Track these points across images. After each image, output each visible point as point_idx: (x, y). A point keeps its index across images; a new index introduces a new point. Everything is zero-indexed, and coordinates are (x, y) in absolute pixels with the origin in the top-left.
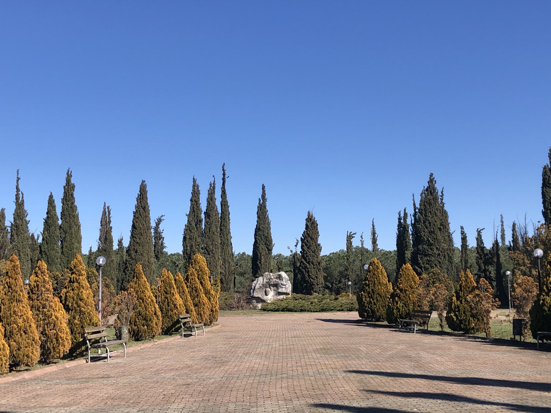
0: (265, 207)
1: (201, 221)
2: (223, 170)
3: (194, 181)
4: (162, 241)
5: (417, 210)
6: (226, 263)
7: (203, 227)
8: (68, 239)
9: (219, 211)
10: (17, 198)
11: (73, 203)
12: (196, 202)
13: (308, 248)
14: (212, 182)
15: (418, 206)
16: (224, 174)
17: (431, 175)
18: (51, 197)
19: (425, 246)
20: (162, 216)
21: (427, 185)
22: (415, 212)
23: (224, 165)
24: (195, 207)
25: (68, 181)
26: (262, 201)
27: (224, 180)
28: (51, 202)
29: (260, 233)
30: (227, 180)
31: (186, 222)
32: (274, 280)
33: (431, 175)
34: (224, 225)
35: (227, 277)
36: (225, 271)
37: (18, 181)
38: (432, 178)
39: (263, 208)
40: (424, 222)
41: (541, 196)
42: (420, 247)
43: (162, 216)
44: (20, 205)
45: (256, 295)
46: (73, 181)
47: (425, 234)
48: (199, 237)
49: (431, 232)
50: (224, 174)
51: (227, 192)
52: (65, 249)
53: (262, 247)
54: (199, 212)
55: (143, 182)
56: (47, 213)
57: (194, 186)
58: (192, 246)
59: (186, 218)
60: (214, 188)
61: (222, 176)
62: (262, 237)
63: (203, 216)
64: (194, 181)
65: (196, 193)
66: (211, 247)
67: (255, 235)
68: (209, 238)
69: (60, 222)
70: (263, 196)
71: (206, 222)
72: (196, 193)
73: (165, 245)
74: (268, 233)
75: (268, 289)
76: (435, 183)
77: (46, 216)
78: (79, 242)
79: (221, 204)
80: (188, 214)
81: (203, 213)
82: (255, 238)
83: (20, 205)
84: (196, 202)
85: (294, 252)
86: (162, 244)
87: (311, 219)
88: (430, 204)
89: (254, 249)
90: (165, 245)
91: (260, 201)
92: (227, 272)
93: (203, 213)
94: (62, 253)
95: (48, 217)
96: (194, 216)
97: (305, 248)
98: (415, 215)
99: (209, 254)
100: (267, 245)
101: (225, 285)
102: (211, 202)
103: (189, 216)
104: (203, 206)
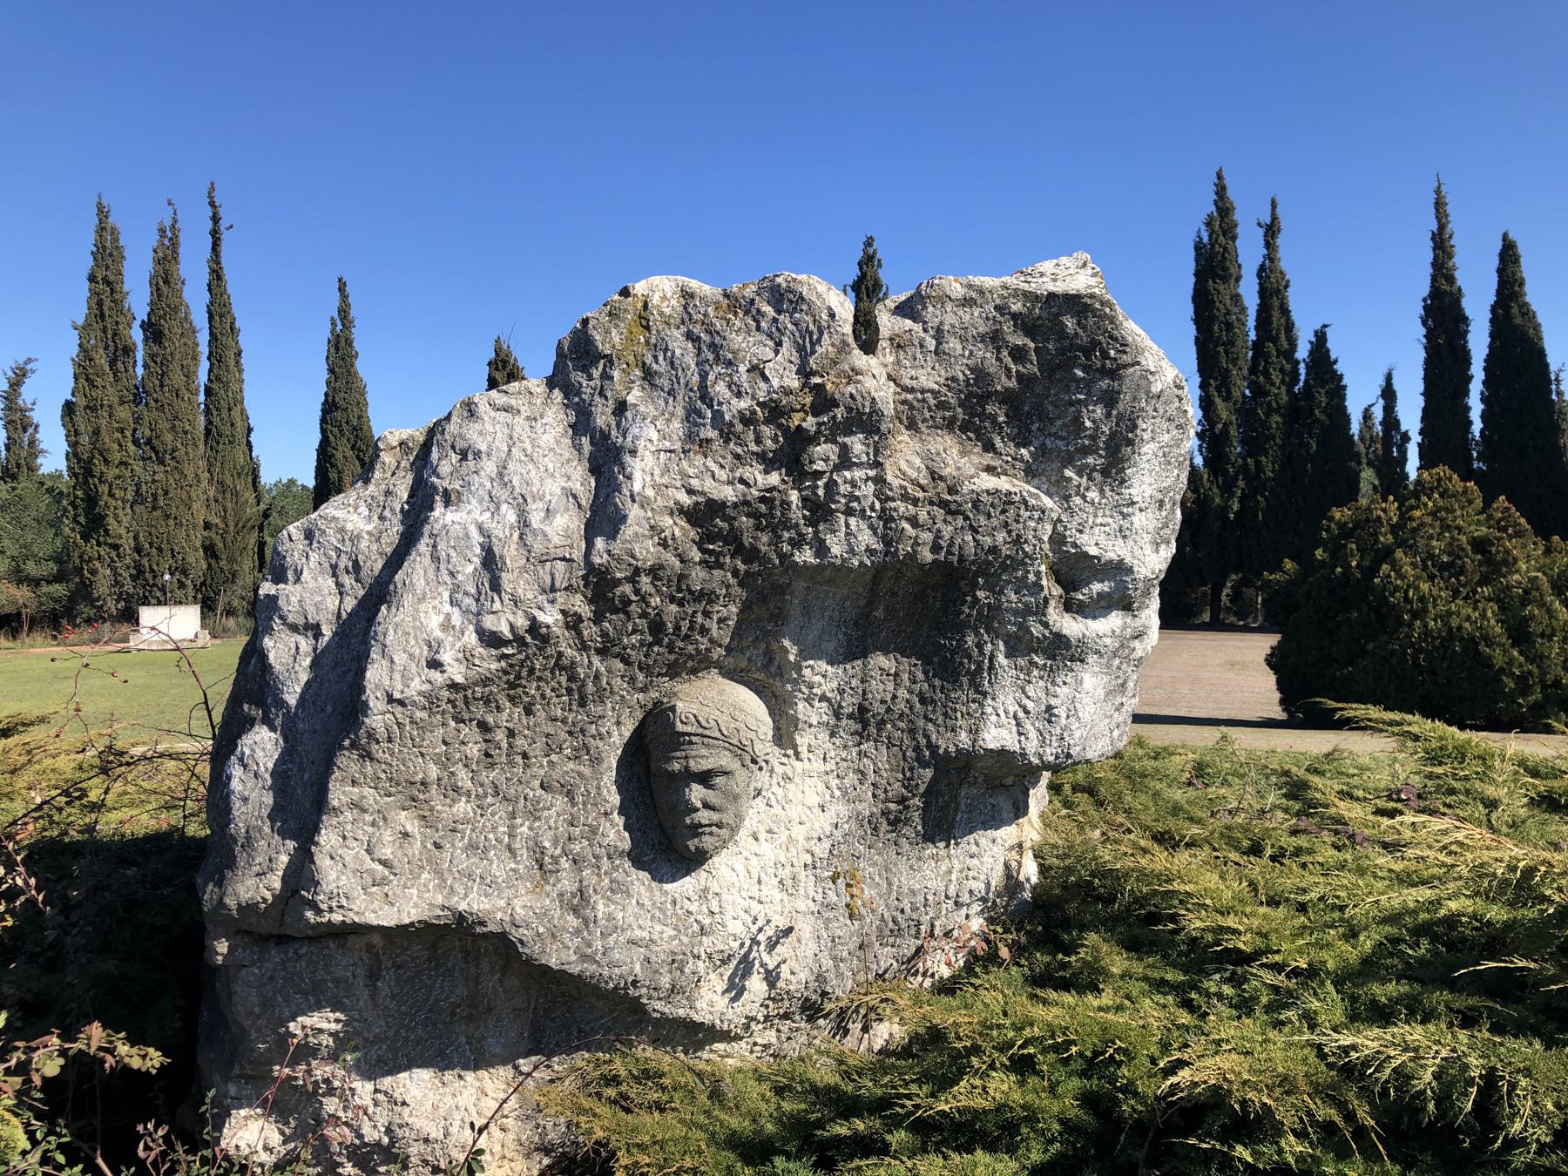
1: (128, 350)
2: (212, 204)
4: (32, 435)
6: (228, 495)
7: (140, 371)
9: (203, 338)
12: (108, 283)
14: (168, 223)
16: (215, 219)
17: (869, 242)
20: (29, 361)
23: (213, 188)
24: (107, 303)
26: (339, 327)
27: (215, 234)
29: (338, 415)
30: (226, 237)
31: (75, 350)
32: (907, 457)
33: (869, 242)
34: (218, 379)
35: (229, 538)
36: (224, 519)
38: (871, 251)
39: (342, 343)
41: (1189, 309)
43: (29, 361)
45: (378, 870)
48: (122, 403)
50: (215, 219)
51: (228, 273)
53: (343, 451)
54: (121, 319)
57: (101, 229)
58: (97, 432)
59: (73, 339)
60: (174, 244)
61: (210, 225)
62: (345, 426)
63: (137, 335)
65: (107, 255)
66: (168, 438)
67: (323, 421)
68: (161, 409)
70: (344, 312)
71: (153, 357)
72: (107, 255)
73: (42, 446)
74: (360, 417)
75: (720, 704)
76: (880, 265)
79: (210, 312)
80: (80, 321)
81: (136, 325)
82: (323, 431)
84: (108, 283)
86: (32, 443)
87: (505, 362)
89: (318, 460)
90: (42, 446)
91: (334, 324)
92: (232, 524)
93: (136, 325)
96: (104, 331)
99: (162, 462)
100: (359, 450)
101: (223, 563)
102: (164, 288)
103: (84, 330)
104: (139, 302)
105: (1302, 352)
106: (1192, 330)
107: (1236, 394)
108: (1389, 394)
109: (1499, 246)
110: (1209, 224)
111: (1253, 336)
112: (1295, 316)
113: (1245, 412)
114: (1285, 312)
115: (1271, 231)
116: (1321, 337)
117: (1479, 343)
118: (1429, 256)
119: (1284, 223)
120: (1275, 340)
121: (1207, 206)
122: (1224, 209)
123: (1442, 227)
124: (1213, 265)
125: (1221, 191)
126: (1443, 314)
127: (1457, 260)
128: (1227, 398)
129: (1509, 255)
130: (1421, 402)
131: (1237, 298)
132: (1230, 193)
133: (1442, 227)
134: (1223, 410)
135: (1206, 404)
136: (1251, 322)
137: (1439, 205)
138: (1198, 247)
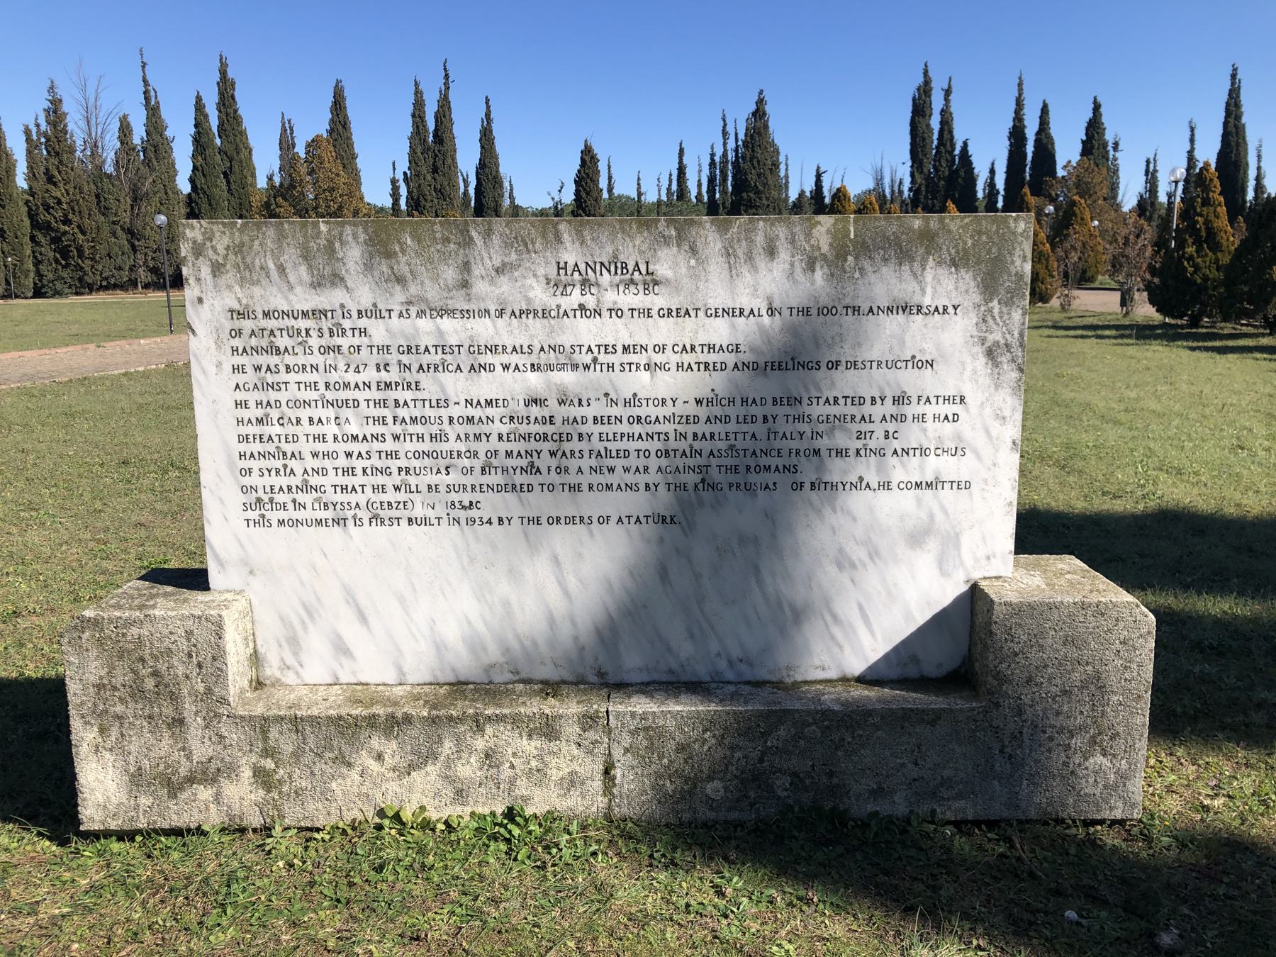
0: (491, 131)
3: (416, 84)
5: (740, 143)
8: (236, 168)
10: (147, 98)
11: (236, 111)
13: (588, 194)
15: (741, 136)
16: (447, 77)
17: (761, 92)
18: (199, 99)
19: (751, 195)
21: (754, 107)
22: (737, 146)
25: (223, 73)
28: (199, 106)
33: (761, 92)
37: (143, 67)
40: (751, 160)
42: (744, 195)
44: (153, 112)
46: (230, 74)
47: (752, 177)
49: (759, 175)
50: (447, 77)
52: (233, 187)
55: (338, 82)
56: (196, 126)
64: (416, 84)
65: (419, 104)
69: (218, 141)
70: (488, 115)
72: (419, 104)
77: (193, 130)
78: (253, 176)
83: (153, 112)
85: (557, 199)
88: (759, 134)
94: (229, 190)
95: (199, 133)
97: (583, 194)
98: (736, 150)
103: (411, 139)
104: (431, 126)
105: (957, 152)
106: (908, 139)
107: (925, 170)
108: (992, 172)
109: (1041, 106)
110: (918, 89)
111: (935, 142)
112: (955, 133)
113: (928, 178)
114: (951, 132)
115: (948, 92)
116: (965, 144)
117: (1030, 149)
118: (1013, 106)
119: (954, 89)
120: (944, 145)
121: (921, 80)
122: (927, 82)
123: (1020, 95)
124: (920, 109)
125: (926, 73)
126: (1017, 135)
127: (1025, 111)
128: (921, 172)
129: (1045, 110)
130: (1004, 176)
131: (928, 125)
132: (930, 74)
133: (1020, 95)
134: (919, 179)
135: (912, 175)
136: (936, 136)
137: (1020, 85)
138: (914, 99)
